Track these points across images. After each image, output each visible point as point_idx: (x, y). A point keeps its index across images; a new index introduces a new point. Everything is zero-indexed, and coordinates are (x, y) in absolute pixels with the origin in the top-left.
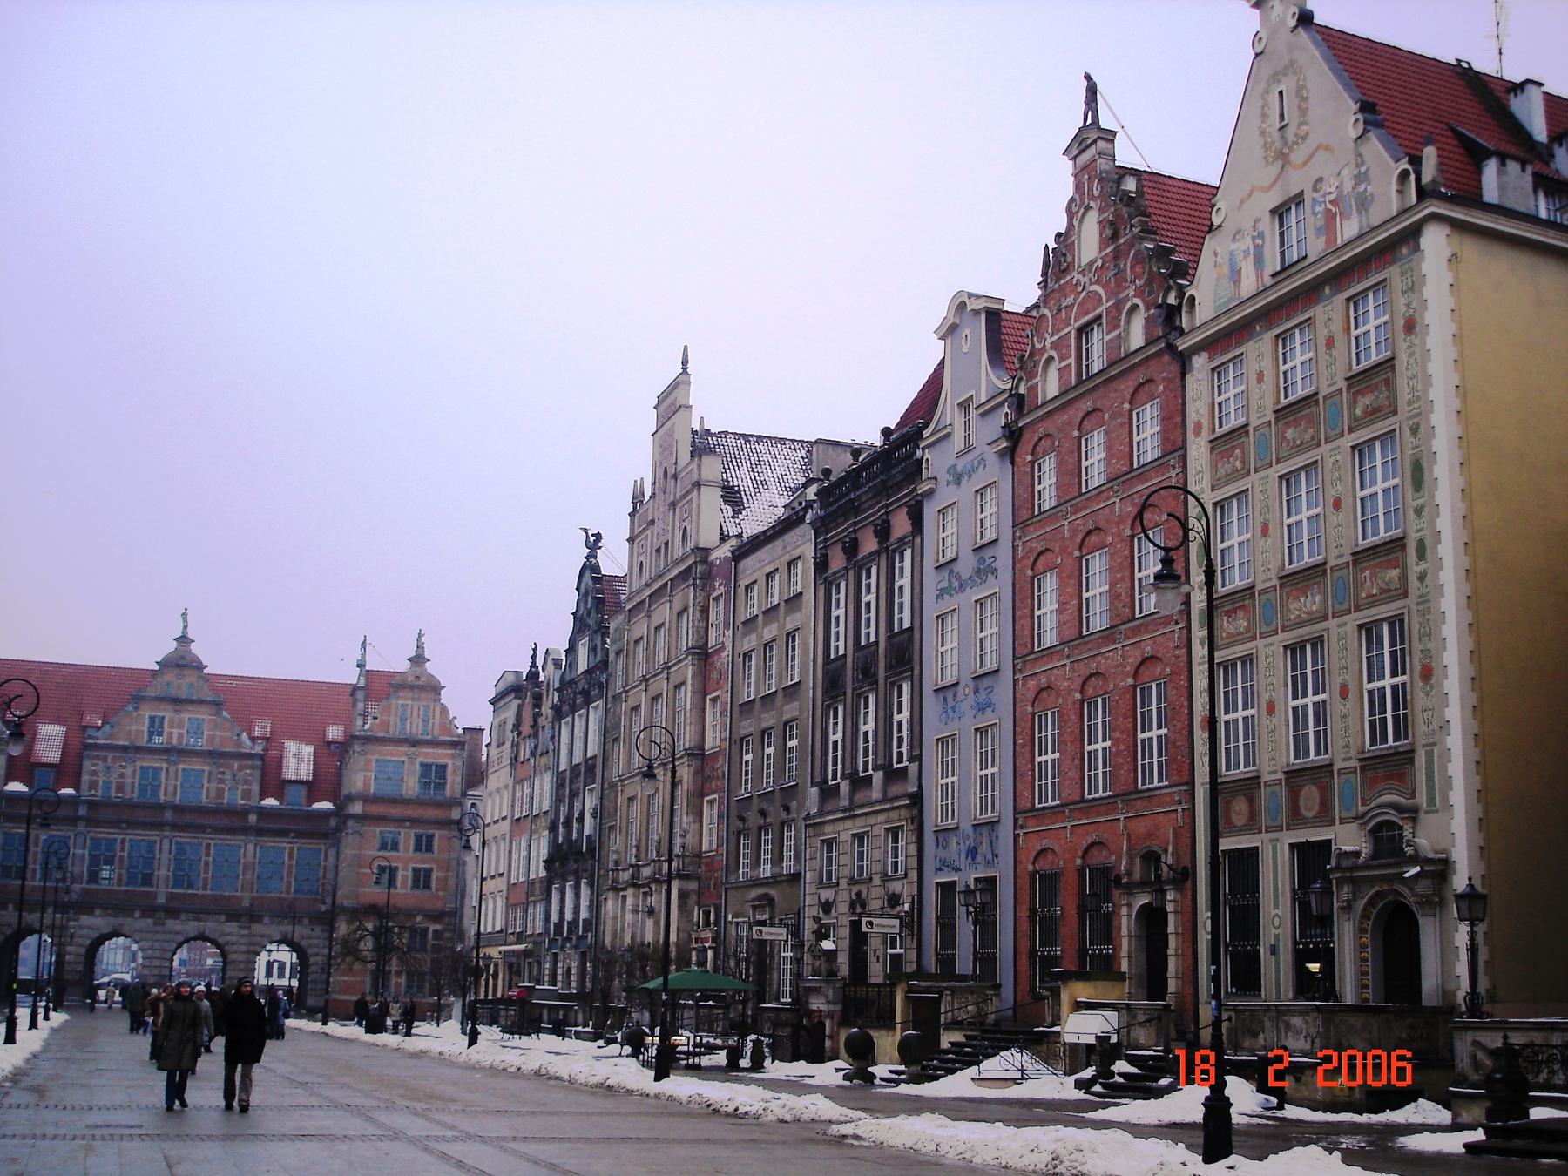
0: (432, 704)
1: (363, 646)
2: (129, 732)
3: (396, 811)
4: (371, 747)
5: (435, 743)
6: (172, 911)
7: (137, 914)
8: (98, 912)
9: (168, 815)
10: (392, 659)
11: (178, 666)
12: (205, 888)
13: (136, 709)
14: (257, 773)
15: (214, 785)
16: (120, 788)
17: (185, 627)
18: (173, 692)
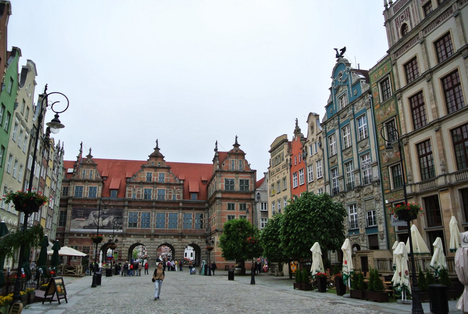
0: (242, 160)
1: (216, 144)
2: (141, 178)
3: (232, 196)
4: (222, 174)
5: (244, 172)
6: (156, 236)
7: (145, 237)
8: (132, 236)
9: (154, 204)
10: (227, 147)
11: (155, 157)
12: (167, 228)
13: (143, 171)
14: (182, 190)
15: (168, 194)
16: (138, 196)
17: (157, 145)
18: (154, 165)
